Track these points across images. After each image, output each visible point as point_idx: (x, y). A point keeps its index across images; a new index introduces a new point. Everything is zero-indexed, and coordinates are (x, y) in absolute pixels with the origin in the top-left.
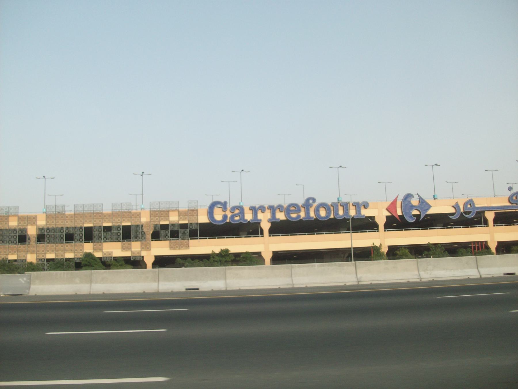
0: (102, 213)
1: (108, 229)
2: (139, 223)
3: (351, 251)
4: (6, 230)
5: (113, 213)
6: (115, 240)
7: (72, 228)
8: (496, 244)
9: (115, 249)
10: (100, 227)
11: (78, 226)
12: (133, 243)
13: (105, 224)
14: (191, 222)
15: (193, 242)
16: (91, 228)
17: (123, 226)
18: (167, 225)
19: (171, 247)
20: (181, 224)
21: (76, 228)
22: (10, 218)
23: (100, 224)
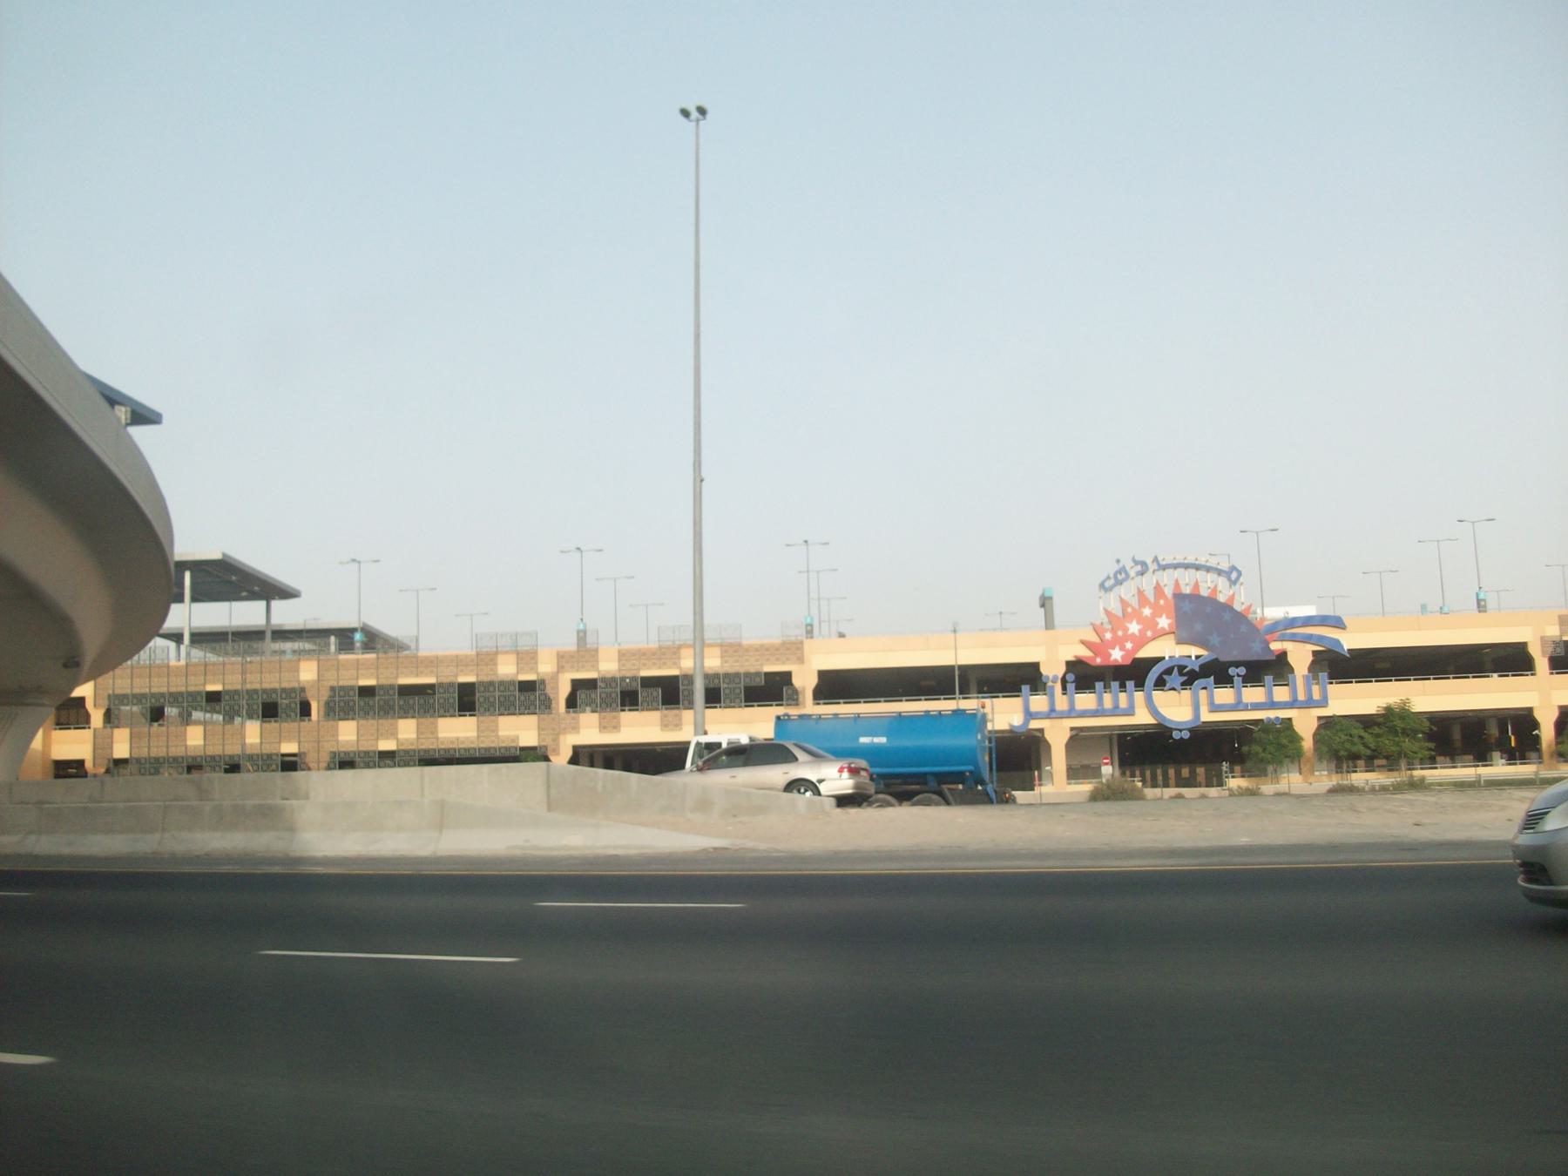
0: (740, 645)
1: (366, 692)
2: (296, 685)
3: (687, 750)
4: (491, 683)
5: (660, 648)
6: (446, 712)
7: (274, 691)
8: (1555, 714)
9: (458, 730)
10: (392, 687)
11: (752, 670)
12: (501, 719)
13: (211, 688)
14: (383, 681)
15: (627, 717)
16: (472, 685)
17: (766, 674)
18: (432, 686)
19: (665, 726)
20: (521, 683)
21: (284, 690)
22: (501, 658)
23: (351, 683)
